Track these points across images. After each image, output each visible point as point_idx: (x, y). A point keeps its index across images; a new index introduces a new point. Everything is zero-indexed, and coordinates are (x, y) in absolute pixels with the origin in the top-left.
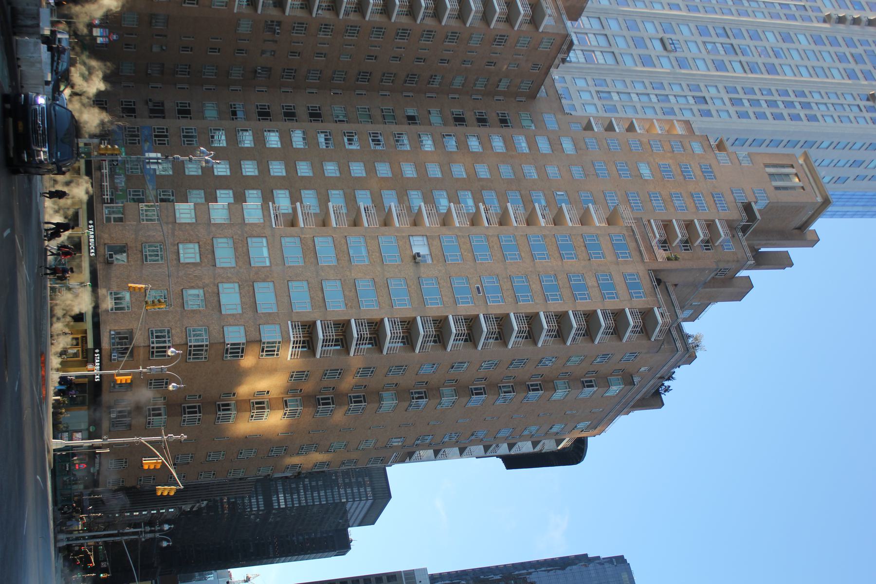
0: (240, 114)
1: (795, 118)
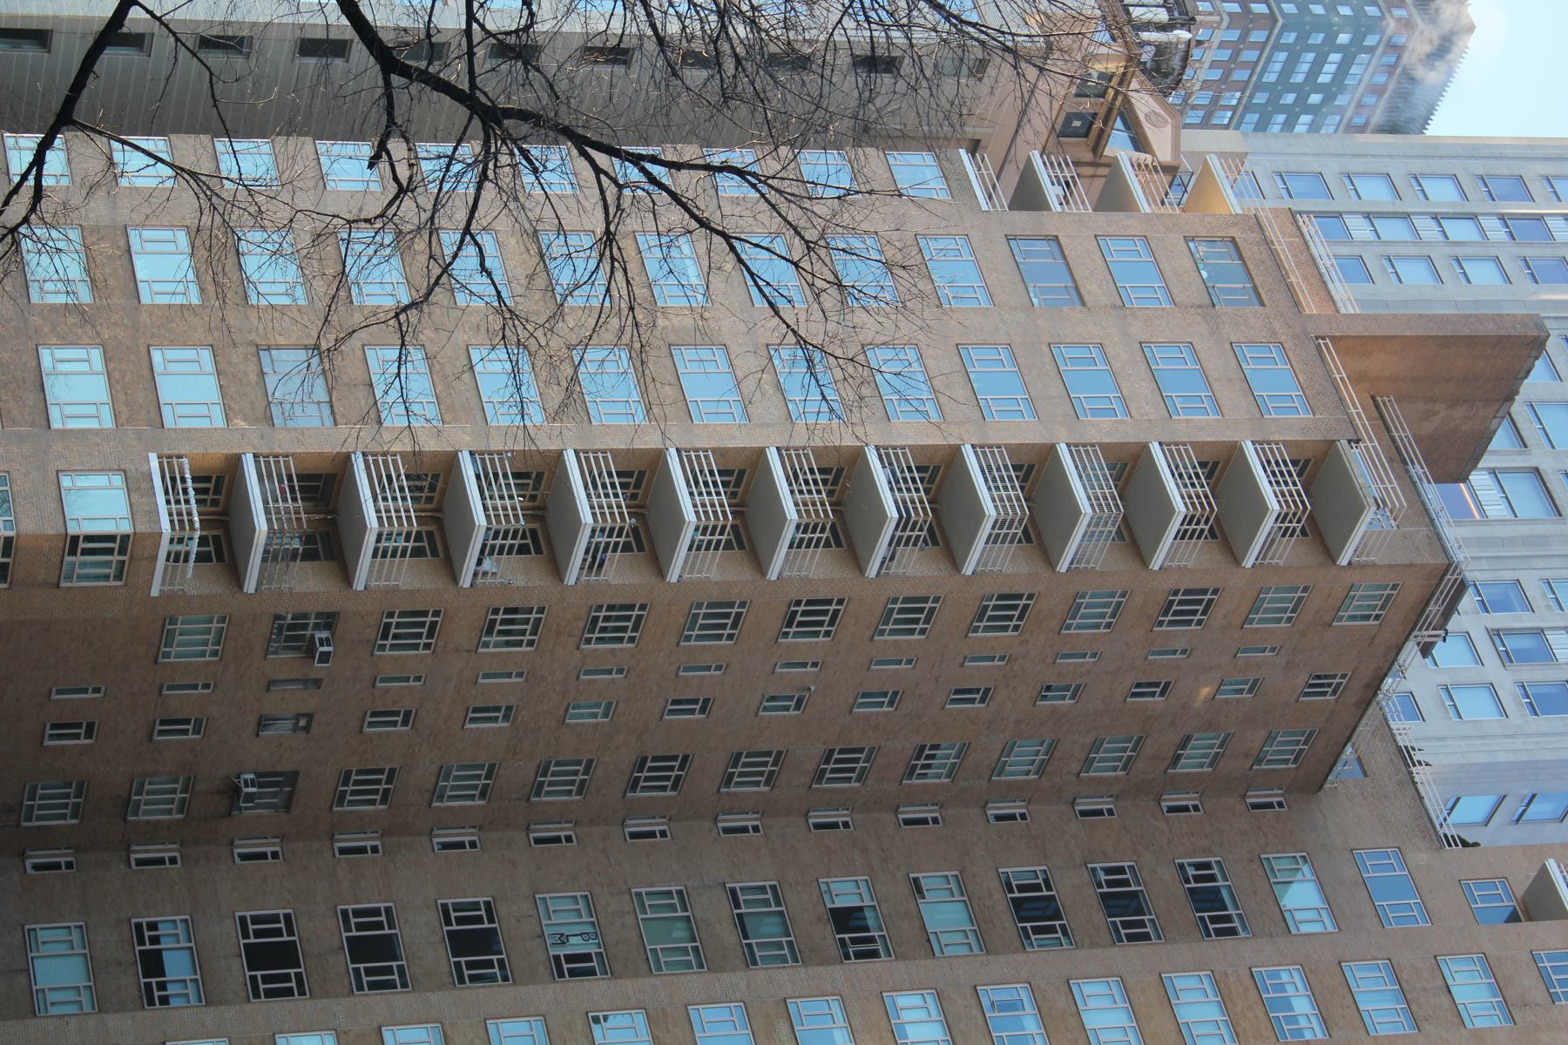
0: (176, 965)
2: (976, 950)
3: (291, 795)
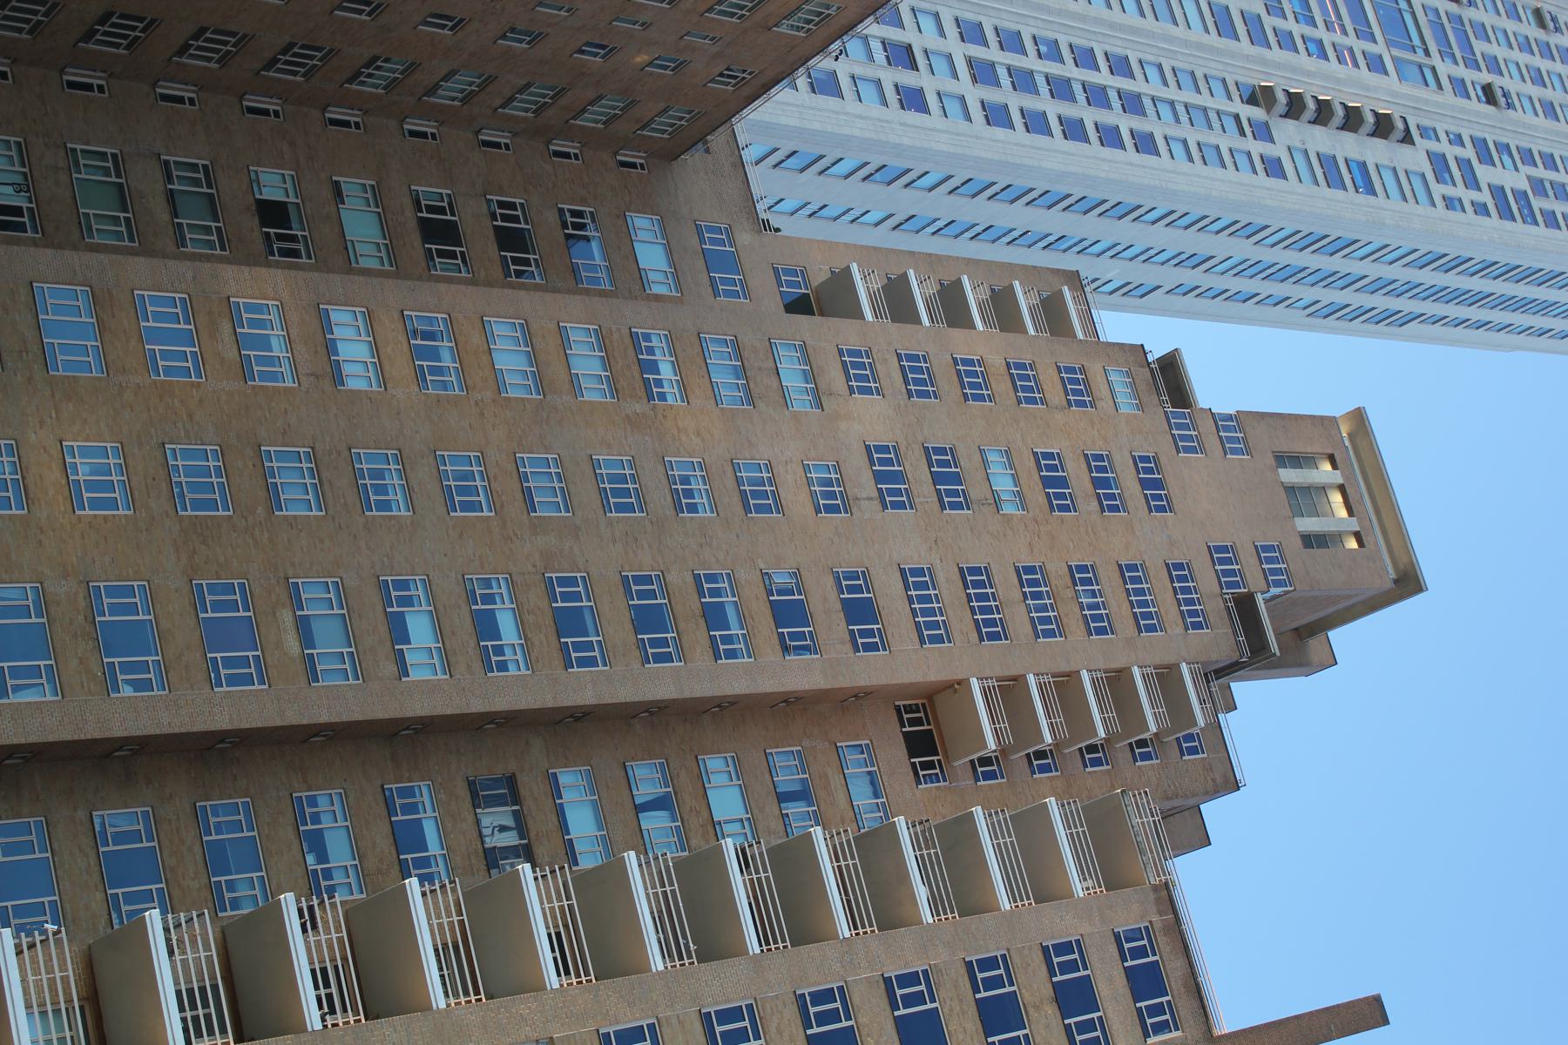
1: (1110, 137)
2: (387, 267)
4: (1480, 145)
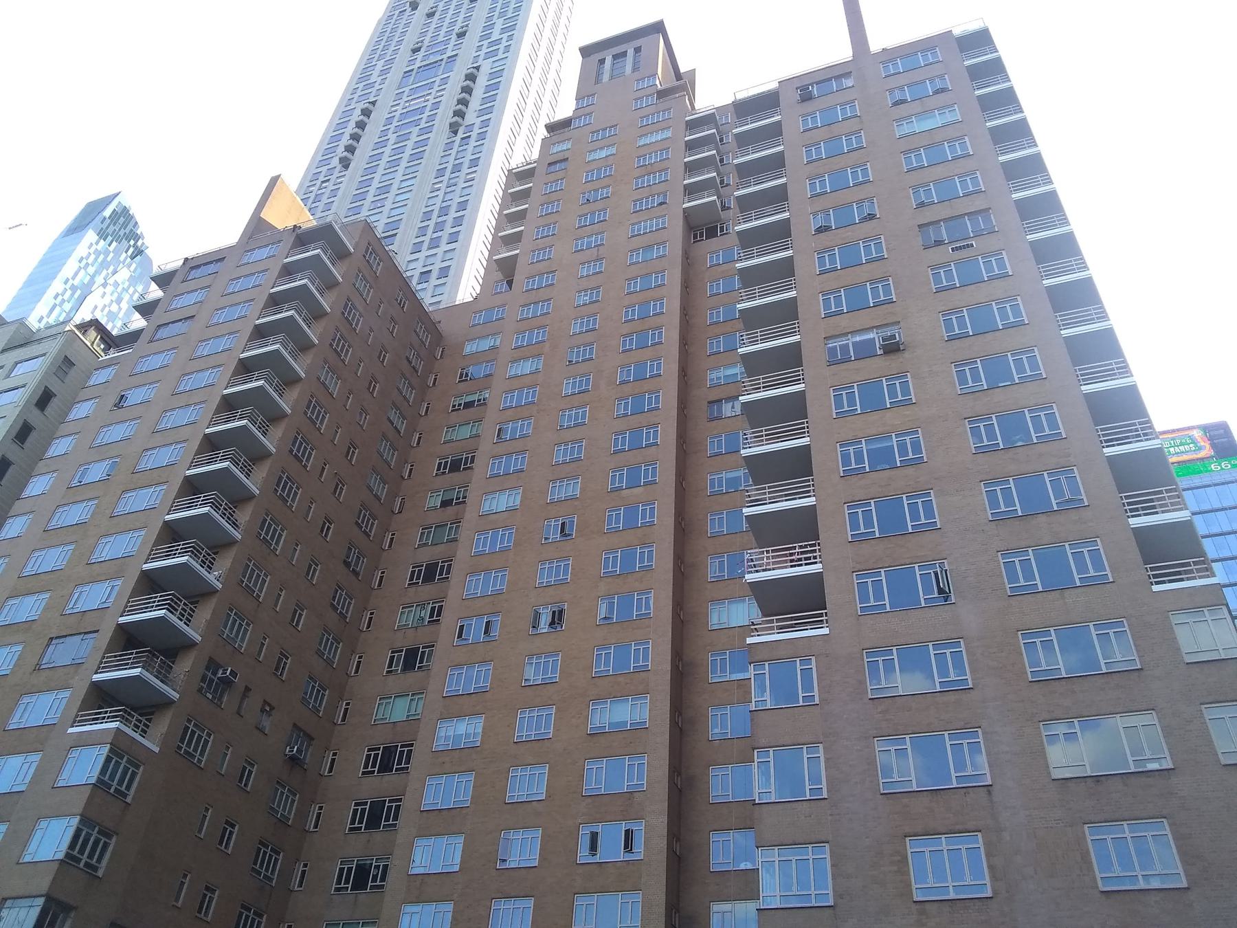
3: (306, 734)
4: (482, 38)
